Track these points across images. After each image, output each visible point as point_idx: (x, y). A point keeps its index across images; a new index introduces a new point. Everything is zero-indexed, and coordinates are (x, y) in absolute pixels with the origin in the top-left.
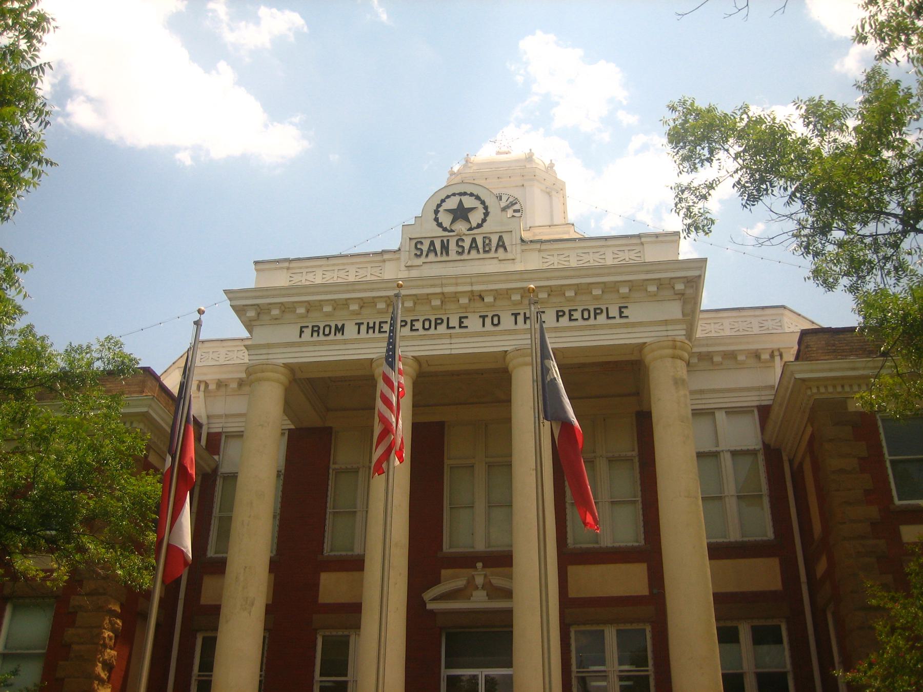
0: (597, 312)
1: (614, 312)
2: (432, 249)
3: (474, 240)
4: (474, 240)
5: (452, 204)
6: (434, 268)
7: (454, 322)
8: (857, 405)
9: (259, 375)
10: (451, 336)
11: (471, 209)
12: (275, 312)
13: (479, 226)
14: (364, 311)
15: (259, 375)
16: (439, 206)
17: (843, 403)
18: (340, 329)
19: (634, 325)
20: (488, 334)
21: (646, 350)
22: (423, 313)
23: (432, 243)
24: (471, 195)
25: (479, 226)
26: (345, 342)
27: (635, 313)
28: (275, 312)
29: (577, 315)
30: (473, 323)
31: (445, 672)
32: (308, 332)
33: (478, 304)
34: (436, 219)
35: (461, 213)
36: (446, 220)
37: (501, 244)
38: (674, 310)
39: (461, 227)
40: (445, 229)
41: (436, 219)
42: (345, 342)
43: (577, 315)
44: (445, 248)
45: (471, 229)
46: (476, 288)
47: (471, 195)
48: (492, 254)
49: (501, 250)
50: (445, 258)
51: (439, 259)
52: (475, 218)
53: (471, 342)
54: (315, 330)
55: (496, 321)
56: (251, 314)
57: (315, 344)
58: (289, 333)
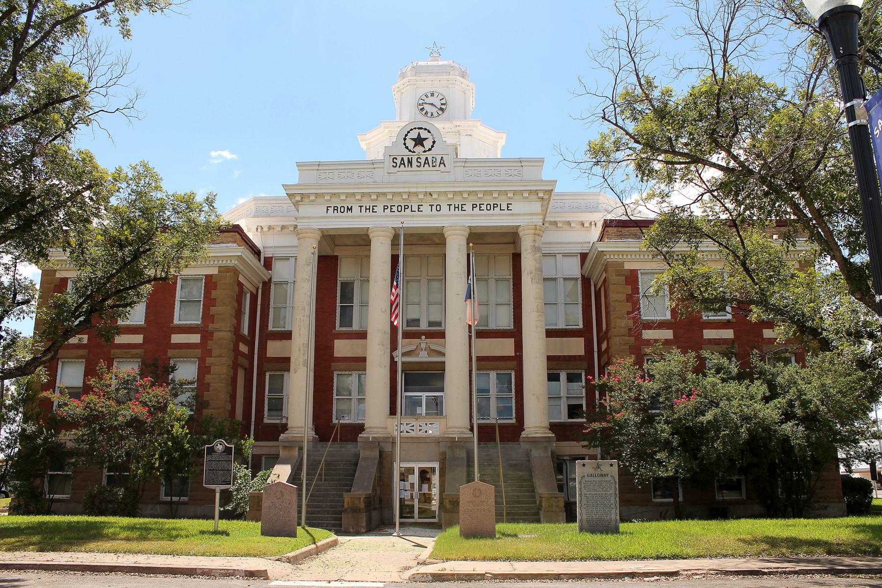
0: (495, 206)
1: (504, 207)
2: (402, 162)
3: (427, 158)
4: (427, 158)
5: (414, 134)
6: (405, 175)
7: (415, 208)
8: (628, 266)
9: (305, 235)
10: (413, 216)
11: (426, 139)
12: (312, 198)
13: (430, 150)
14: (363, 199)
15: (305, 235)
16: (406, 135)
17: (622, 264)
18: (350, 209)
19: (512, 215)
20: (434, 216)
21: (520, 229)
22: (397, 201)
23: (402, 159)
24: (425, 129)
25: (430, 150)
26: (353, 217)
27: (516, 207)
28: (312, 198)
29: (484, 207)
30: (426, 208)
31: (424, 395)
32: (331, 210)
33: (429, 197)
34: (405, 144)
35: (419, 141)
36: (410, 144)
37: (442, 163)
38: (537, 207)
39: (419, 149)
40: (410, 151)
41: (405, 144)
42: (353, 217)
43: (484, 207)
44: (410, 162)
45: (425, 152)
46: (428, 190)
47: (425, 129)
48: (437, 168)
49: (442, 165)
50: (410, 169)
51: (407, 169)
52: (428, 144)
53: (422, 220)
54: (336, 209)
55: (439, 208)
56: (298, 198)
57: (336, 217)
58: (321, 210)
